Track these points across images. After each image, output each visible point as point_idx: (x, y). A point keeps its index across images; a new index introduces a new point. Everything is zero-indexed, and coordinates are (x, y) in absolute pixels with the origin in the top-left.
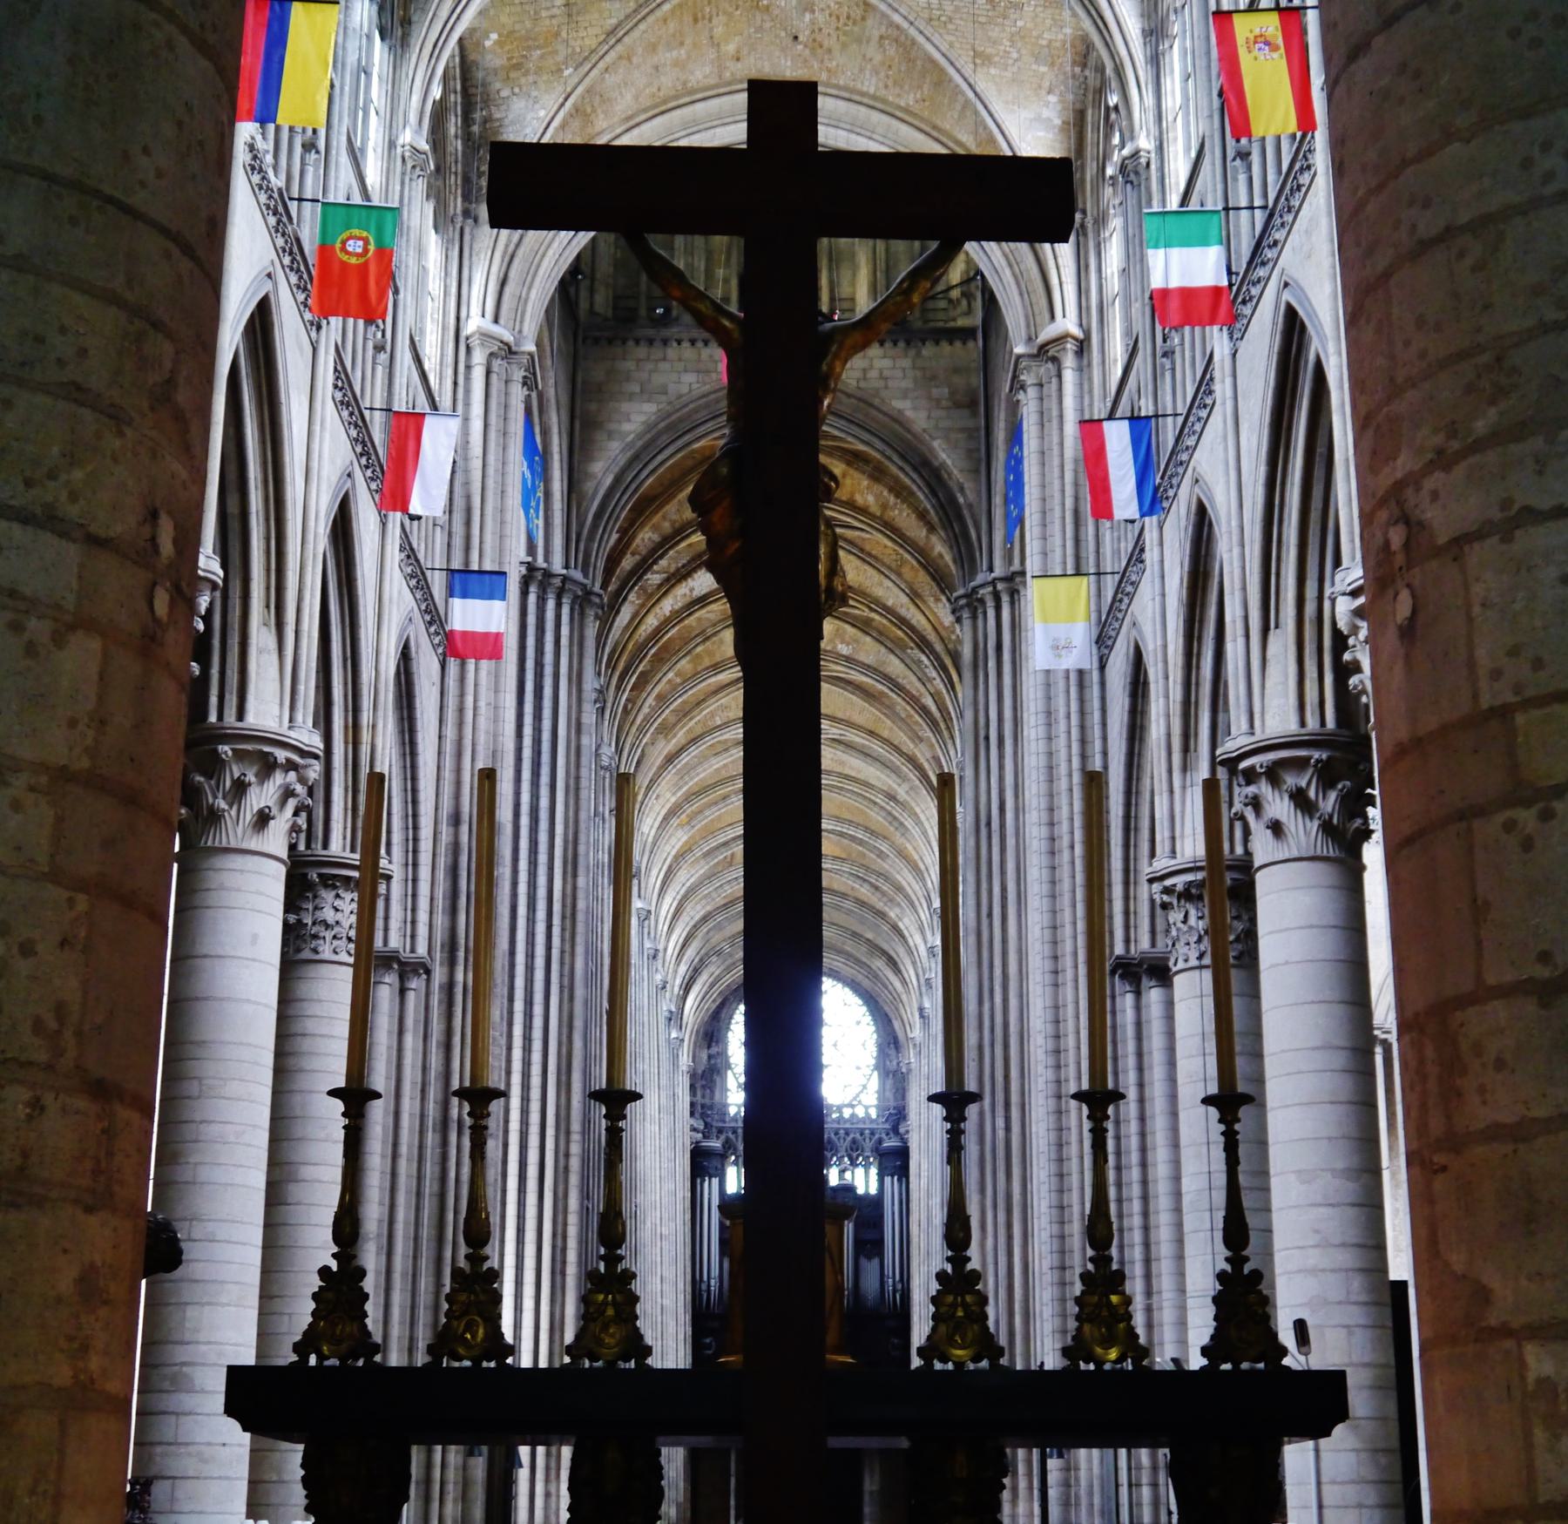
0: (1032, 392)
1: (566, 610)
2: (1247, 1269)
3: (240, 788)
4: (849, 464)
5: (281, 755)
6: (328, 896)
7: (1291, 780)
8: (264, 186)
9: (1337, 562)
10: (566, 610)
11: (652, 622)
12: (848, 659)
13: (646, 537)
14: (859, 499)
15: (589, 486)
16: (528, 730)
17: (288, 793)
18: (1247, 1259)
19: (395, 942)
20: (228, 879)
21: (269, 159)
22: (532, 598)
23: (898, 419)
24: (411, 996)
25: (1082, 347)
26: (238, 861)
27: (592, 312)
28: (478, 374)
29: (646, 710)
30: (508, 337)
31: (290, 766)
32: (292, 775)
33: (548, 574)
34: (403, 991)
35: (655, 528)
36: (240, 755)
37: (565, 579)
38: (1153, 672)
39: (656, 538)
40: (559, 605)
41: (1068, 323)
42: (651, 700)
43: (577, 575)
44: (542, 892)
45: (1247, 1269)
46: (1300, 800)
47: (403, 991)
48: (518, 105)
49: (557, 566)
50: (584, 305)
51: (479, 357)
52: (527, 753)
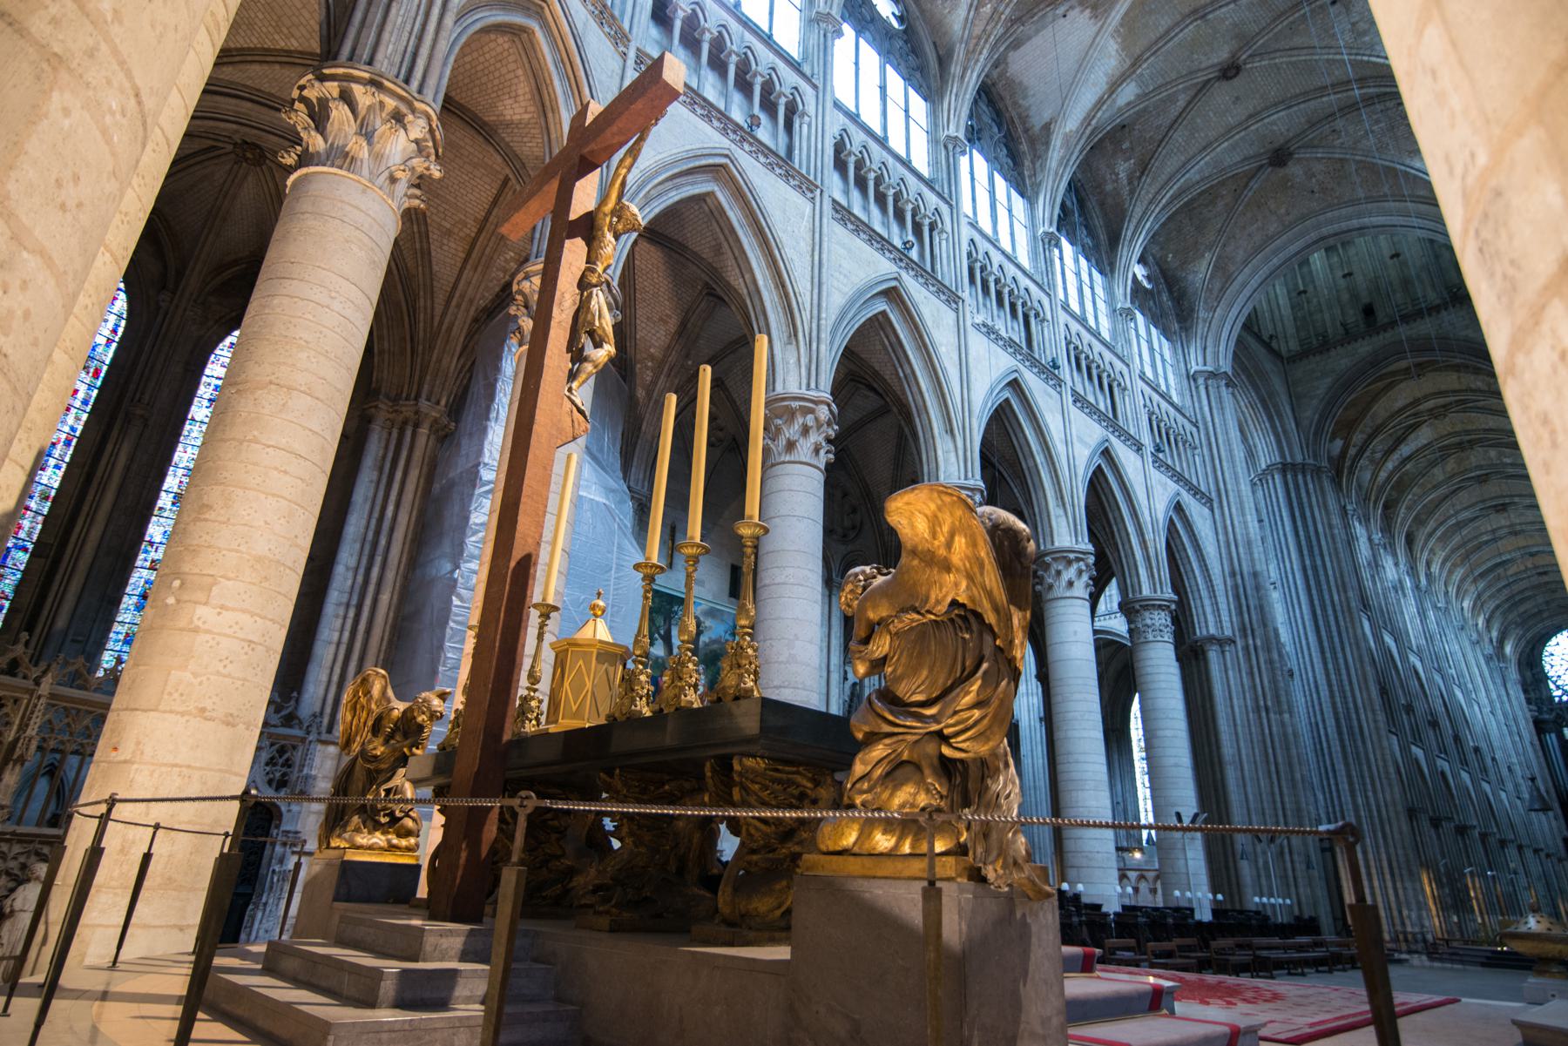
1: (1309, 478)
3: (1059, 573)
4: (1458, 371)
5: (1072, 556)
6: (1147, 614)
10: (1309, 478)
11: (1383, 475)
12: (1511, 464)
13: (1358, 438)
14: (1473, 386)
15: (1306, 423)
16: (1301, 533)
17: (1080, 572)
19: (1212, 631)
20: (1061, 611)
22: (1289, 477)
24: (1227, 654)
26: (1062, 603)
27: (1289, 351)
28: (1202, 388)
29: (1402, 515)
30: (1210, 369)
31: (1078, 560)
32: (1081, 563)
33: (1293, 465)
34: (1223, 652)
35: (1362, 432)
37: (1304, 465)
39: (1365, 436)
40: (1304, 476)
42: (1403, 510)
43: (1311, 461)
44: (1328, 602)
47: (1223, 652)
48: (1190, 277)
49: (1299, 459)
51: (1201, 381)
52: (1303, 543)
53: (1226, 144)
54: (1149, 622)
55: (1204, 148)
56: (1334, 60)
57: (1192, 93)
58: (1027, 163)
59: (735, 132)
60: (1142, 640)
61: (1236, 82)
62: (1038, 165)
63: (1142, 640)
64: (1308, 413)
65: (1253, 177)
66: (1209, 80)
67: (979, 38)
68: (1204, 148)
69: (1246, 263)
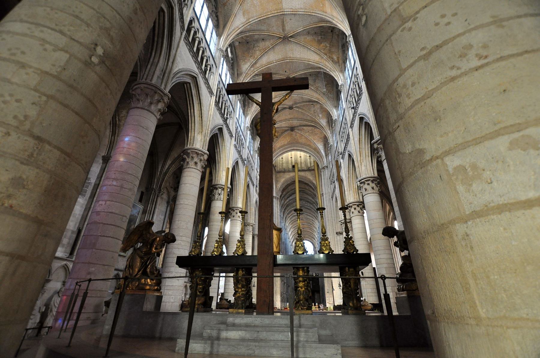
0: (322, 172)
2: (349, 237)
6: (248, 227)
7: (354, 207)
8: (237, 149)
9: (357, 178)
15: (278, 187)
18: (349, 235)
21: (238, 146)
23: (309, 179)
25: (327, 167)
36: (236, 209)
38: (338, 199)
41: (326, 165)
45: (349, 237)
46: (355, 209)
50: (276, 169)
53: (284, 122)
54: (248, 229)
55: (280, 121)
56: (309, 115)
57: (282, 108)
58: (246, 107)
59: (200, 70)
60: (246, 233)
61: (290, 110)
62: (249, 109)
63: (246, 233)
64: (279, 185)
65: (286, 131)
66: (286, 108)
67: (249, 74)
68: (280, 121)
69: (279, 148)
